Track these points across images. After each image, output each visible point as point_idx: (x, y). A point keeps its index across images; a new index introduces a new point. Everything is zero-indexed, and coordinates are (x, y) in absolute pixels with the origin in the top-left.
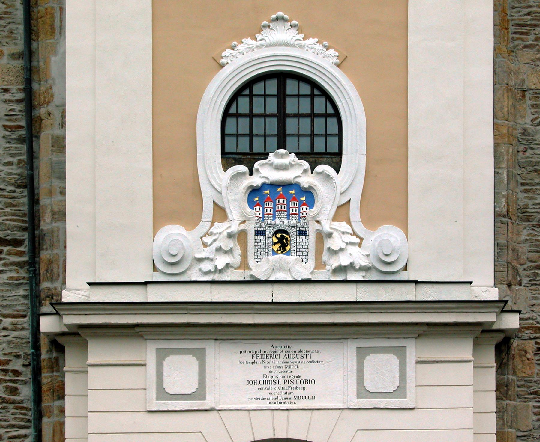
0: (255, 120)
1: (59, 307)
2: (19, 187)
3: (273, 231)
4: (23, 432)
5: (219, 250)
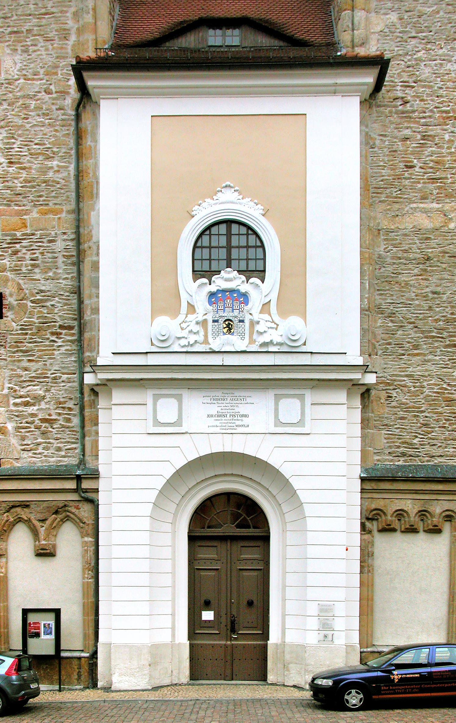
1: (95, 368)
2: (72, 293)
3: (223, 320)
4: (74, 446)
5: (191, 332)
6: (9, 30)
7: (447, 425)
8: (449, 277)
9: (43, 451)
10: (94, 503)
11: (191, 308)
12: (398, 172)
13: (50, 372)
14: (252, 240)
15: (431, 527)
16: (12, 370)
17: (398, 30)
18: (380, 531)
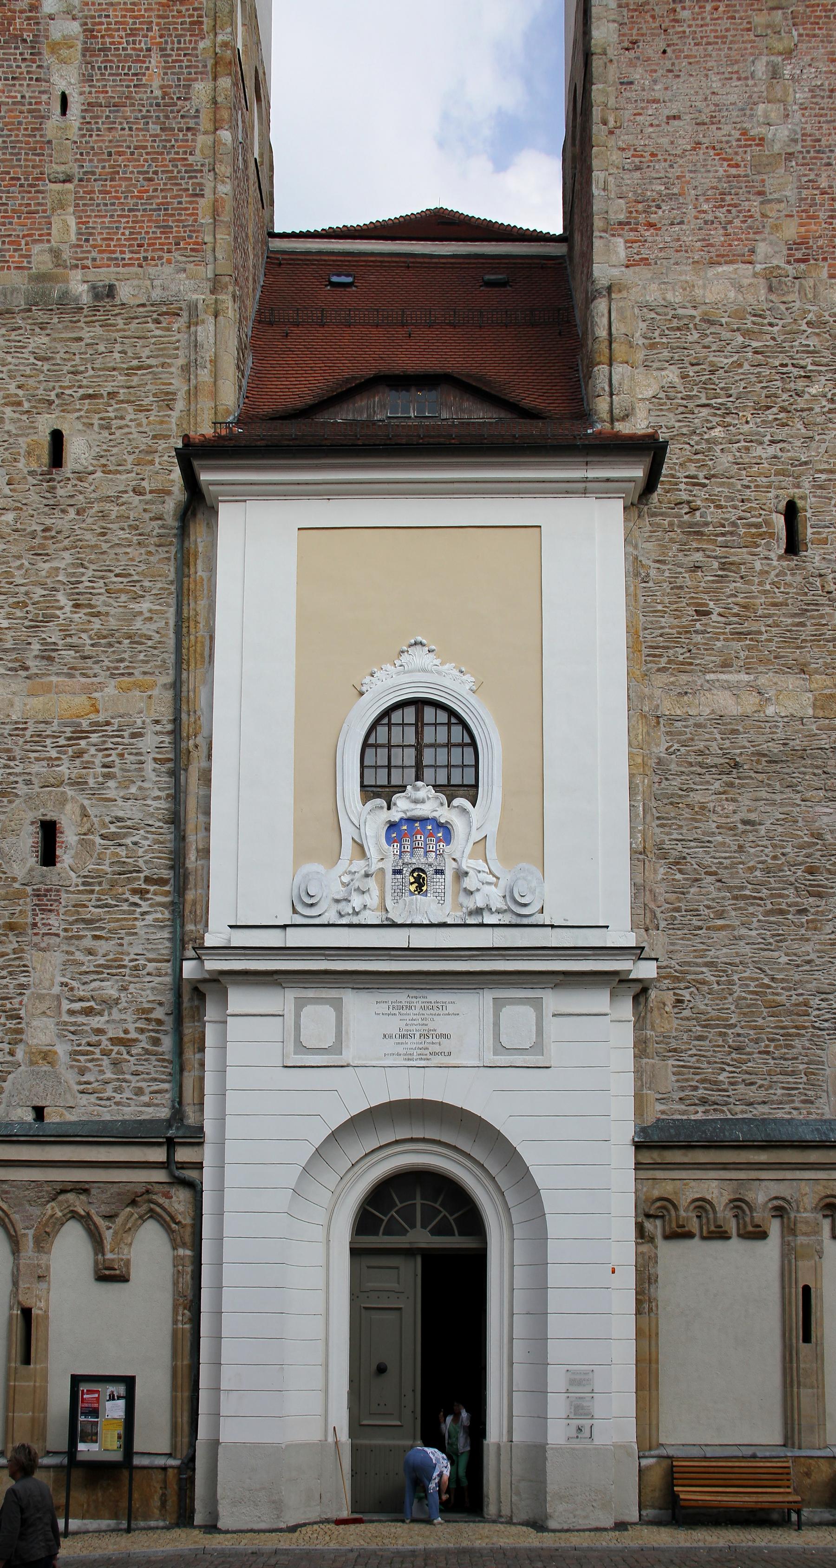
0: (393, 750)
1: (201, 951)
6: (81, 391)
7: (771, 1049)
8: (769, 796)
9: (114, 1094)
10: (195, 1188)
11: (360, 849)
12: (685, 621)
13: (127, 958)
14: (457, 732)
15: (750, 1228)
16: (67, 952)
17: (680, 395)
18: (667, 1237)
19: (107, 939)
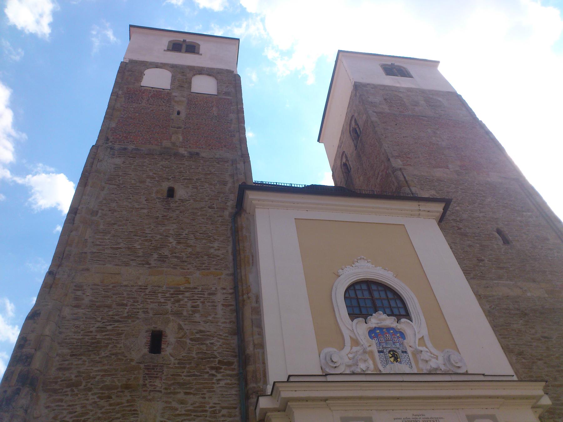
16: (166, 402)
19: (194, 394)
